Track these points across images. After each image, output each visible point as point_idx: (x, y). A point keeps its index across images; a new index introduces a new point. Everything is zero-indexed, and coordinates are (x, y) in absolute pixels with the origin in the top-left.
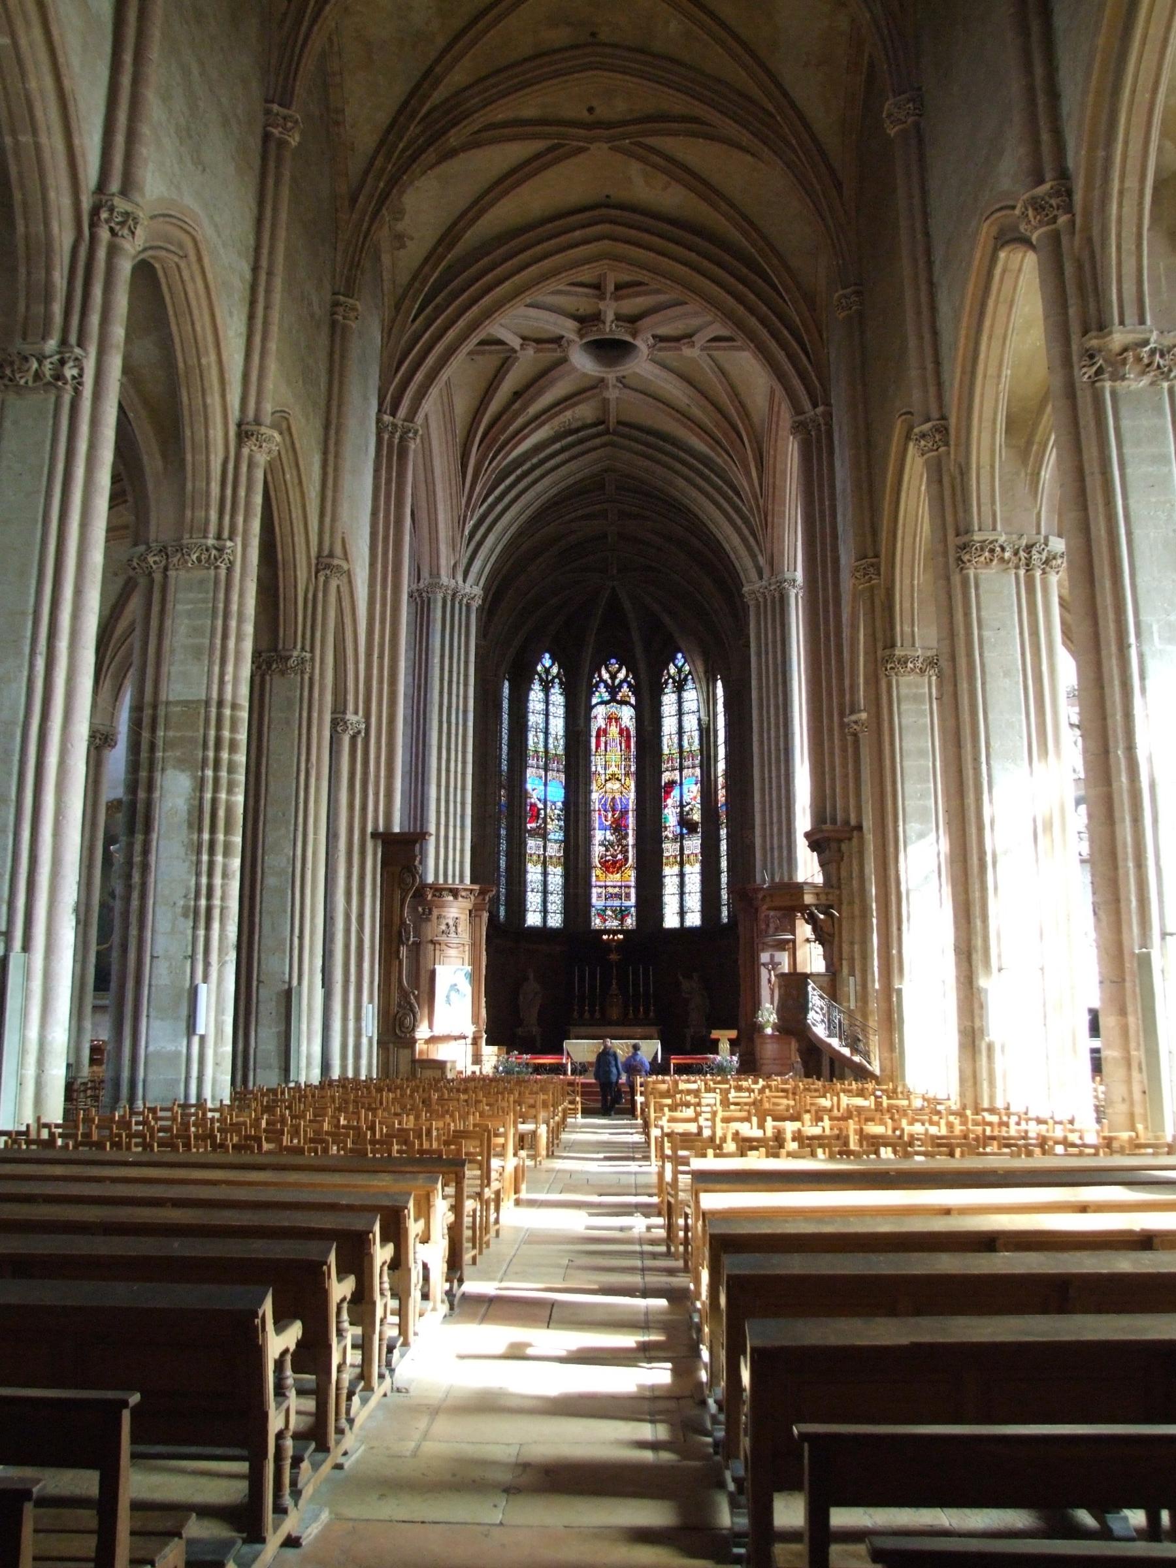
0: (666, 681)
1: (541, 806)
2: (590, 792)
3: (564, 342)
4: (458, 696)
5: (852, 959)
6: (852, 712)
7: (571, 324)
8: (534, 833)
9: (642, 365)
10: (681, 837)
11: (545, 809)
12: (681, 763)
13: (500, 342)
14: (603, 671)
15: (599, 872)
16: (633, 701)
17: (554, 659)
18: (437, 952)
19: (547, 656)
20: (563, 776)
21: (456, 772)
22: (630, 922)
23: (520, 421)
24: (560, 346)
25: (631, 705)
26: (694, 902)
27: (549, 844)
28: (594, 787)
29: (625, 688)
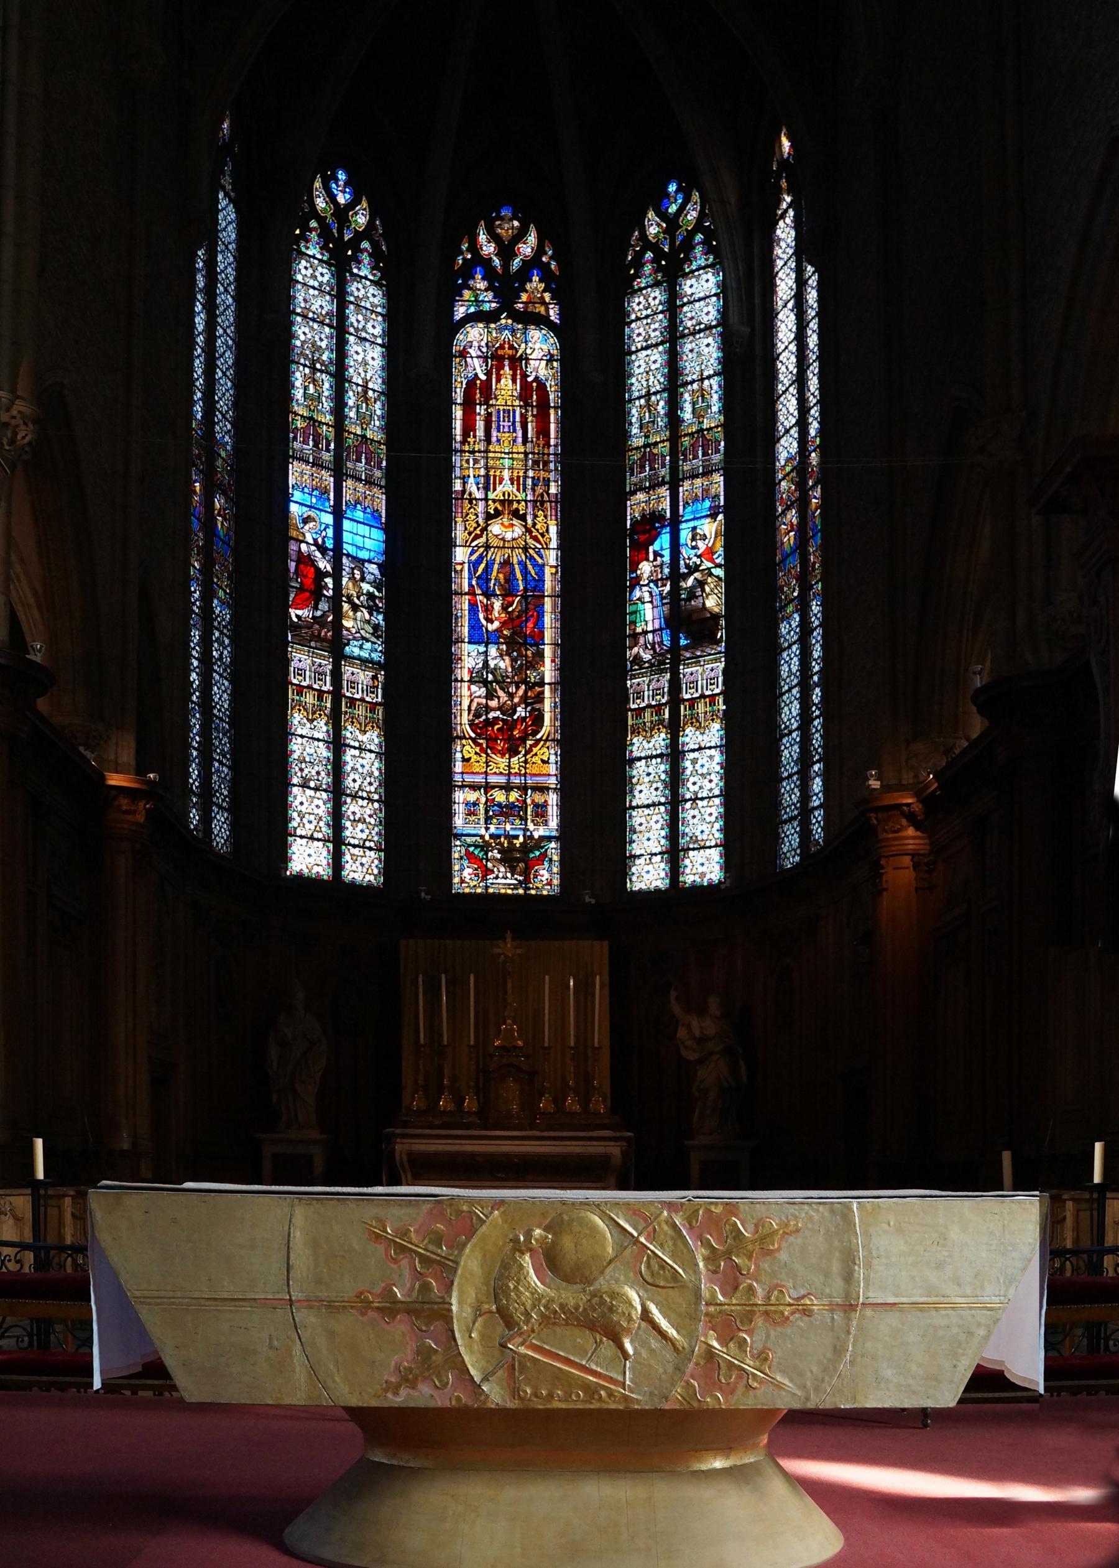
2: (450, 544)
20: (381, 502)
27: (348, 671)
28: (459, 534)
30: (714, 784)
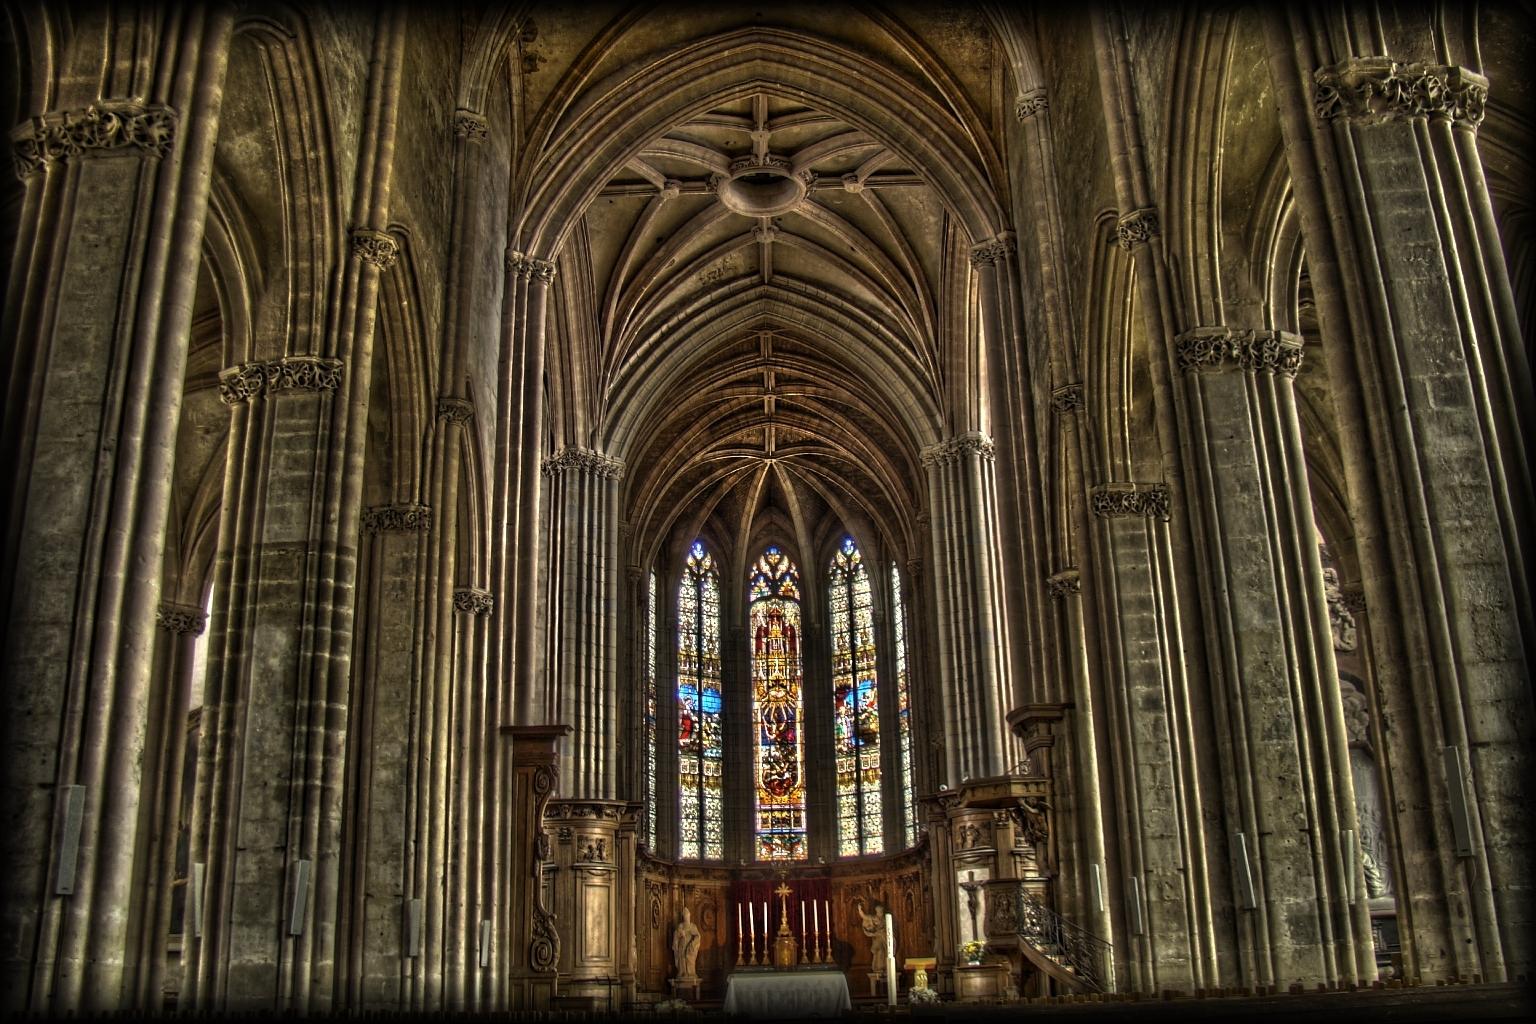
0: (834, 572)
1: (695, 718)
2: (750, 701)
3: (712, 180)
4: (599, 582)
5: (1069, 861)
6: (1056, 571)
7: (719, 158)
8: (689, 750)
9: (798, 204)
10: (855, 751)
11: (700, 722)
12: (854, 665)
13: (643, 181)
14: (763, 563)
15: (763, 794)
16: (797, 595)
17: (705, 551)
18: (579, 881)
19: (699, 547)
21: (598, 670)
22: (801, 851)
23: (664, 271)
24: (709, 183)
25: (795, 600)
26: (875, 824)
27: (706, 763)
28: (755, 696)
29: (788, 582)
30: (877, 808)
